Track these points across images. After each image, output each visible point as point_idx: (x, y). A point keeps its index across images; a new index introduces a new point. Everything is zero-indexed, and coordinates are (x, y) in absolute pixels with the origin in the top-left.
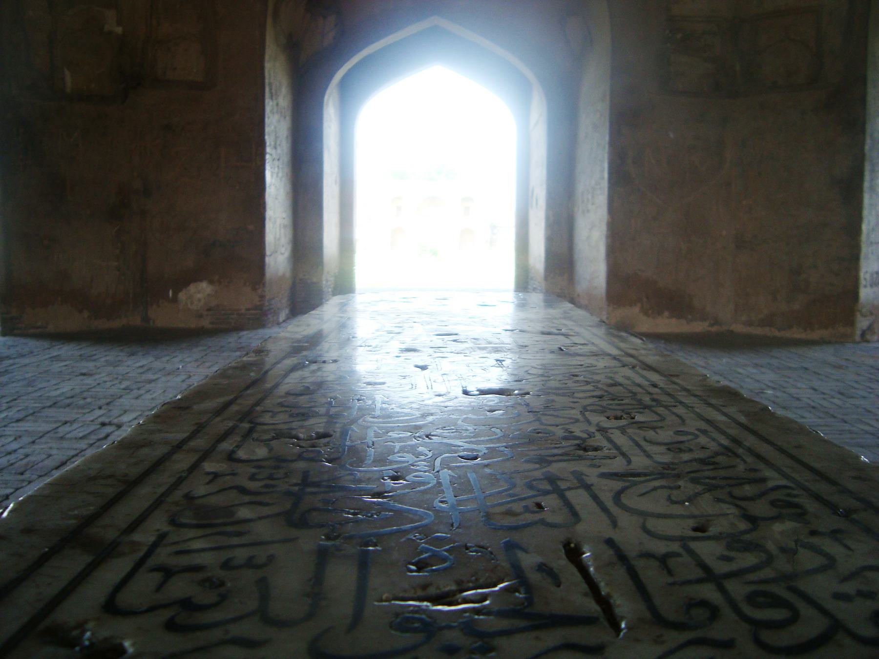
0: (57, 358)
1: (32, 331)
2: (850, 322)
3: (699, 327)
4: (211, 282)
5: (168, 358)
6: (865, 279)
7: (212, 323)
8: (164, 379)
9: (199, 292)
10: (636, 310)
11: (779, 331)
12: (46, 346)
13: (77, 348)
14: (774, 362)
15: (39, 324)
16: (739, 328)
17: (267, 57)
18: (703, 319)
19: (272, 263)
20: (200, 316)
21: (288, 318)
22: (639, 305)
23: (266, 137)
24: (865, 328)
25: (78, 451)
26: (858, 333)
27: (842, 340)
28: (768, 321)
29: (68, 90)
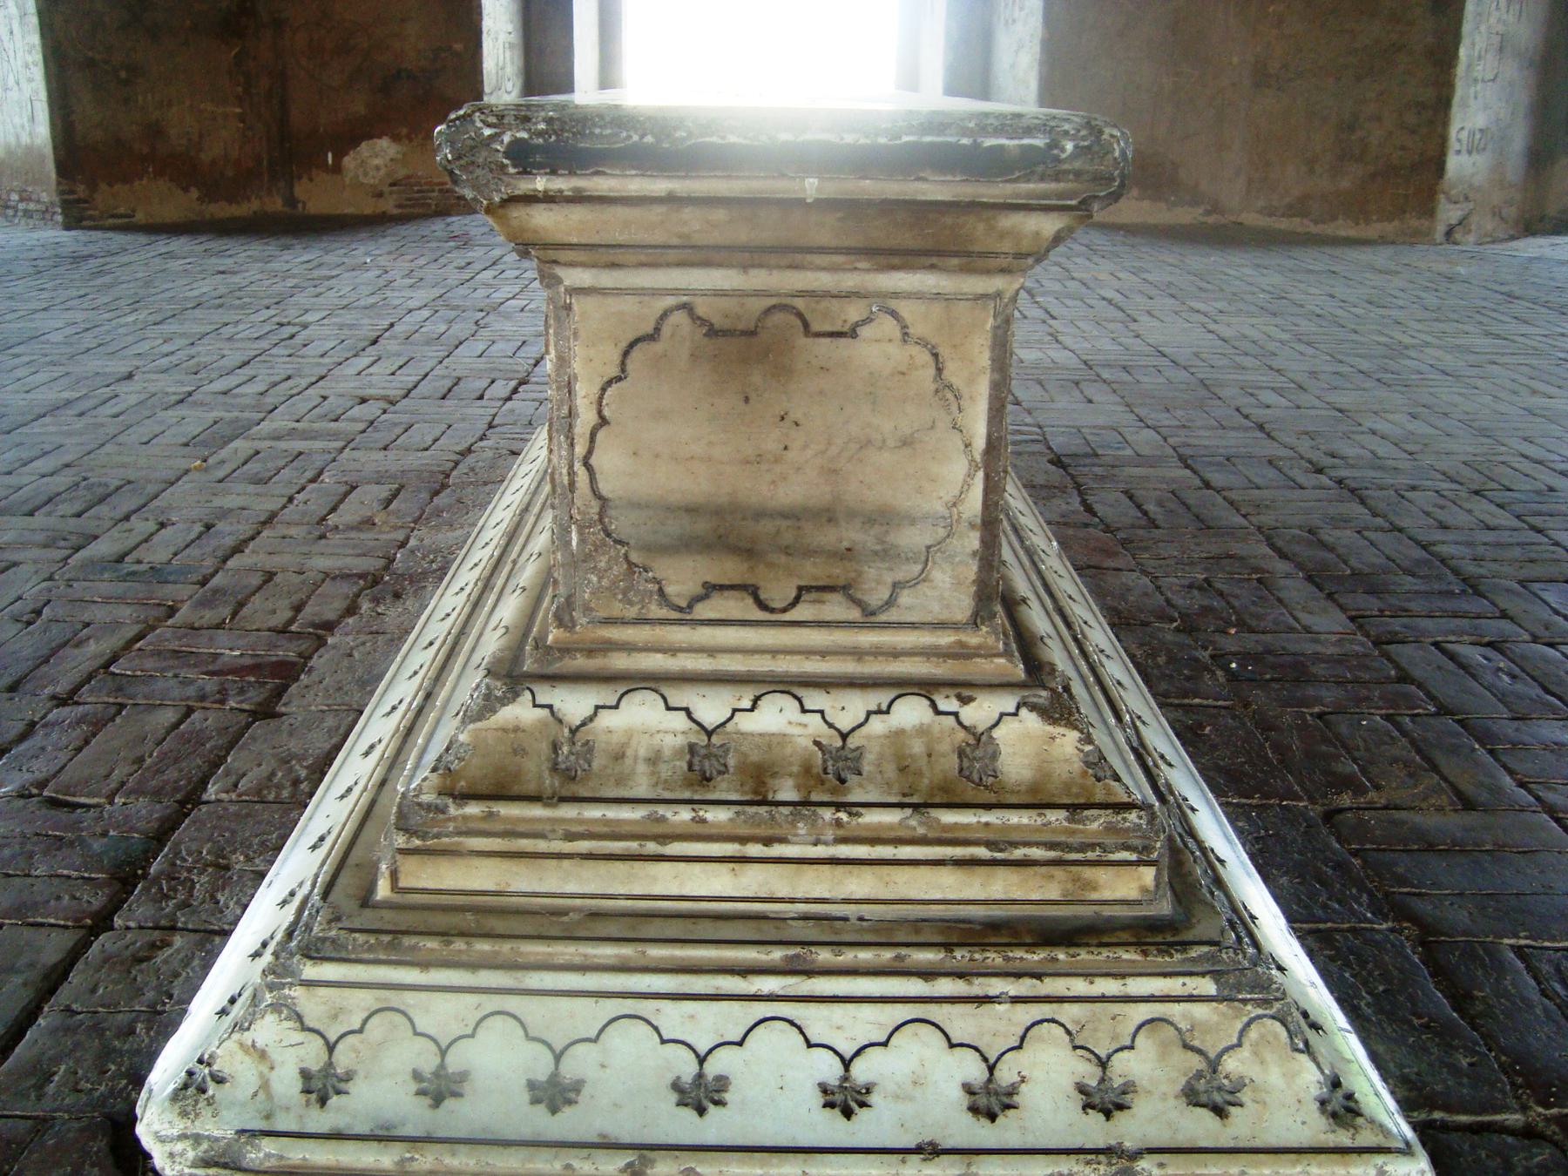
0: (170, 255)
2: (1429, 211)
4: (396, 138)
5: (343, 251)
6: (1459, 141)
7: (399, 206)
8: (347, 275)
9: (376, 156)
12: (145, 242)
14: (1289, 263)
15: (122, 210)
16: (1251, 219)
18: (1195, 203)
20: (380, 195)
24: (1454, 222)
26: (1441, 229)
27: (1415, 237)
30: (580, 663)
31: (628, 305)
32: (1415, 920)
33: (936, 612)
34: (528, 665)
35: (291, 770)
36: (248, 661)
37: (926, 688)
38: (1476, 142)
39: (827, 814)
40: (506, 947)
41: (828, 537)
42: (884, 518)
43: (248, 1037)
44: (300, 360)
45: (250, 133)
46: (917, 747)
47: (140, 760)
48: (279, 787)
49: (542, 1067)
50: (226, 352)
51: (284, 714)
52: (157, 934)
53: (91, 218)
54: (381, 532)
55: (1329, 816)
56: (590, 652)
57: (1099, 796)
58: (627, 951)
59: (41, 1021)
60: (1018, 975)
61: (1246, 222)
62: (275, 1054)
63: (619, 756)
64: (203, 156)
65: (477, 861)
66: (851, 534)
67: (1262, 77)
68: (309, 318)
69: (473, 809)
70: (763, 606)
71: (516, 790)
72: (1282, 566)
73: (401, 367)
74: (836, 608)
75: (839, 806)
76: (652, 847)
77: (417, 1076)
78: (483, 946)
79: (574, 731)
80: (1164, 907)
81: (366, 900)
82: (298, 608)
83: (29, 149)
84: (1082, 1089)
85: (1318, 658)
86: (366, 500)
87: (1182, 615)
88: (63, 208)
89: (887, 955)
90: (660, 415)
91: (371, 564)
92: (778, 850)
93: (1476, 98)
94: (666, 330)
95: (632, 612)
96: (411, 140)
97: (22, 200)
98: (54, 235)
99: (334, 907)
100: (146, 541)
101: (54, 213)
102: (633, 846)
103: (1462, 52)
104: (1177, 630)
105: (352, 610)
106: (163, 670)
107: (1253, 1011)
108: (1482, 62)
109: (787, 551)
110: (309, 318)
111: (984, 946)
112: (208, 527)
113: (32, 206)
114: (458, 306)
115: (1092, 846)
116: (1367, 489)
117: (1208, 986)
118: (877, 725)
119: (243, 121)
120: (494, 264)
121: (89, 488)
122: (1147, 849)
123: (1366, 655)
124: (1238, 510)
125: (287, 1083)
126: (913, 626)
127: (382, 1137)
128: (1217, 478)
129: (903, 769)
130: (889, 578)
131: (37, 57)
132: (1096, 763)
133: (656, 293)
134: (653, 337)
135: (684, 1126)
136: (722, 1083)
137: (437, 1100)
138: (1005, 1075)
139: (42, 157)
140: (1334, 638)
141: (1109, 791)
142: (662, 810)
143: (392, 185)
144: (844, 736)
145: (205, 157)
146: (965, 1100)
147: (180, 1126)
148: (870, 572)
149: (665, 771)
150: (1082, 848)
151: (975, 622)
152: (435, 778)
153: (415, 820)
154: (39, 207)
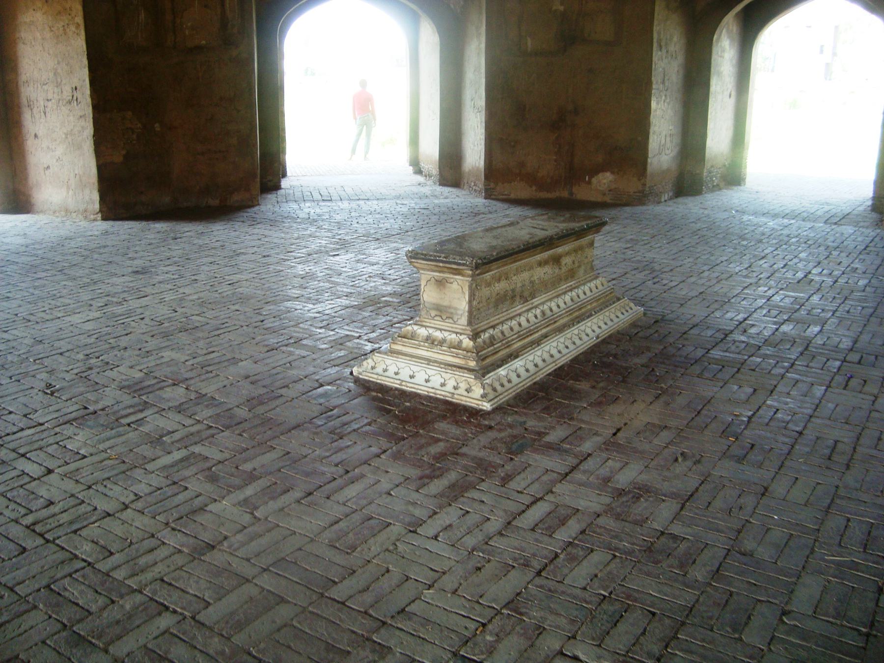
1: (501, 197)
4: (613, 173)
15: (506, 193)
17: (656, 22)
20: (604, 194)
21: (671, 199)
23: (653, 79)
29: (529, 50)
30: (419, 323)
33: (462, 323)
37: (457, 333)
41: (450, 310)
42: (456, 309)
53: (495, 195)
64: (539, 174)
66: (452, 311)
74: (451, 321)
98: (480, 201)
113: (477, 188)
118: (449, 337)
125: (370, 367)
127: (377, 374)
131: (483, 137)
135: (409, 379)
151: (468, 325)
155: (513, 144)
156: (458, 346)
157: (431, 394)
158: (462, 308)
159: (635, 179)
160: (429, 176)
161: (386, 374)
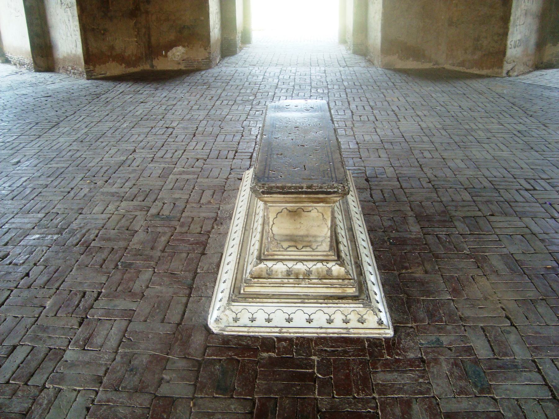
2: (501, 67)
3: (427, 66)
4: (184, 46)
6: (511, 45)
7: (185, 67)
10: (396, 57)
11: (467, 69)
13: (128, 86)
15: (103, 72)
16: (448, 67)
18: (430, 61)
19: (213, 35)
20: (179, 64)
22: (397, 55)
25: (165, 140)
26: (505, 72)
28: (462, 64)
30: (270, 257)
31: (277, 208)
32: (408, 295)
33: (324, 250)
34: (262, 258)
35: (212, 266)
36: (196, 241)
37: (321, 261)
38: (517, 44)
39: (307, 280)
40: (261, 300)
41: (307, 239)
42: (315, 236)
43: (225, 313)
44: (177, 143)
45: (139, 46)
46: (320, 270)
47: (183, 264)
48: (211, 270)
49: (267, 317)
50: (156, 140)
51: (206, 254)
52: (200, 297)
53: (94, 76)
54: (213, 205)
55: (399, 274)
56: (272, 255)
57: (347, 278)
58: (278, 300)
59: (187, 311)
60: (334, 304)
61: (446, 68)
62: (229, 315)
63: (277, 272)
64: (126, 54)
65: (256, 287)
66: (311, 239)
67: (451, 23)
68: (174, 124)
69: (256, 280)
70: (297, 249)
71: (262, 277)
72: (411, 213)
73: (204, 146)
74: (308, 249)
75: (309, 279)
76: (282, 285)
77: (249, 318)
78: (258, 300)
79: (270, 268)
80: (357, 294)
81: (240, 293)
82: (202, 228)
83: (75, 55)
84: (343, 320)
85: (410, 239)
86: (208, 194)
87: (385, 228)
88: (86, 73)
89: (315, 301)
90: (282, 222)
91: (214, 215)
92: (300, 285)
93: (517, 31)
94: (283, 211)
95: (278, 250)
96: (188, 47)
97: (72, 69)
98: (84, 82)
99: (235, 294)
100: (162, 208)
101: (83, 75)
102: (279, 285)
103: (512, 18)
104: (383, 232)
105: (213, 228)
106: (181, 243)
107: (368, 309)
108: (519, 20)
109: (301, 241)
110: (174, 124)
111: (329, 299)
112: (174, 204)
113: (76, 71)
114: (213, 119)
115: (345, 285)
116: (439, 188)
117: (362, 306)
118: (314, 267)
119: (137, 42)
120: (219, 97)
121: (143, 191)
122: (354, 285)
123: (420, 238)
124: (406, 195)
125: (231, 320)
126: (320, 251)
128: (404, 185)
129: (318, 273)
130: (316, 245)
131: (78, 28)
132: (347, 273)
133: (281, 206)
134: (281, 212)
135: (287, 325)
136: (292, 319)
137: (252, 322)
138: (332, 318)
139: (79, 58)
140: (415, 233)
141: (349, 277)
142: (283, 280)
143: (183, 60)
144: (309, 269)
145: (126, 54)
146: (326, 321)
147: (216, 325)
148: (314, 244)
149: (283, 274)
150: (344, 285)
151: (329, 251)
152: (250, 275)
153: (247, 282)
154: (78, 72)
155: (102, 32)
156: (328, 275)
157: (323, 335)
158: (323, 234)
159: (202, 49)
160: (22, 64)
161: (255, 324)
